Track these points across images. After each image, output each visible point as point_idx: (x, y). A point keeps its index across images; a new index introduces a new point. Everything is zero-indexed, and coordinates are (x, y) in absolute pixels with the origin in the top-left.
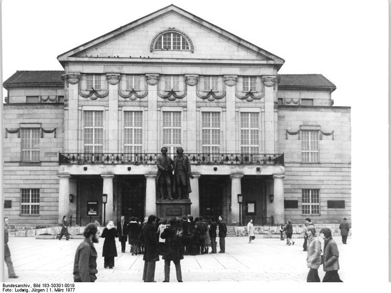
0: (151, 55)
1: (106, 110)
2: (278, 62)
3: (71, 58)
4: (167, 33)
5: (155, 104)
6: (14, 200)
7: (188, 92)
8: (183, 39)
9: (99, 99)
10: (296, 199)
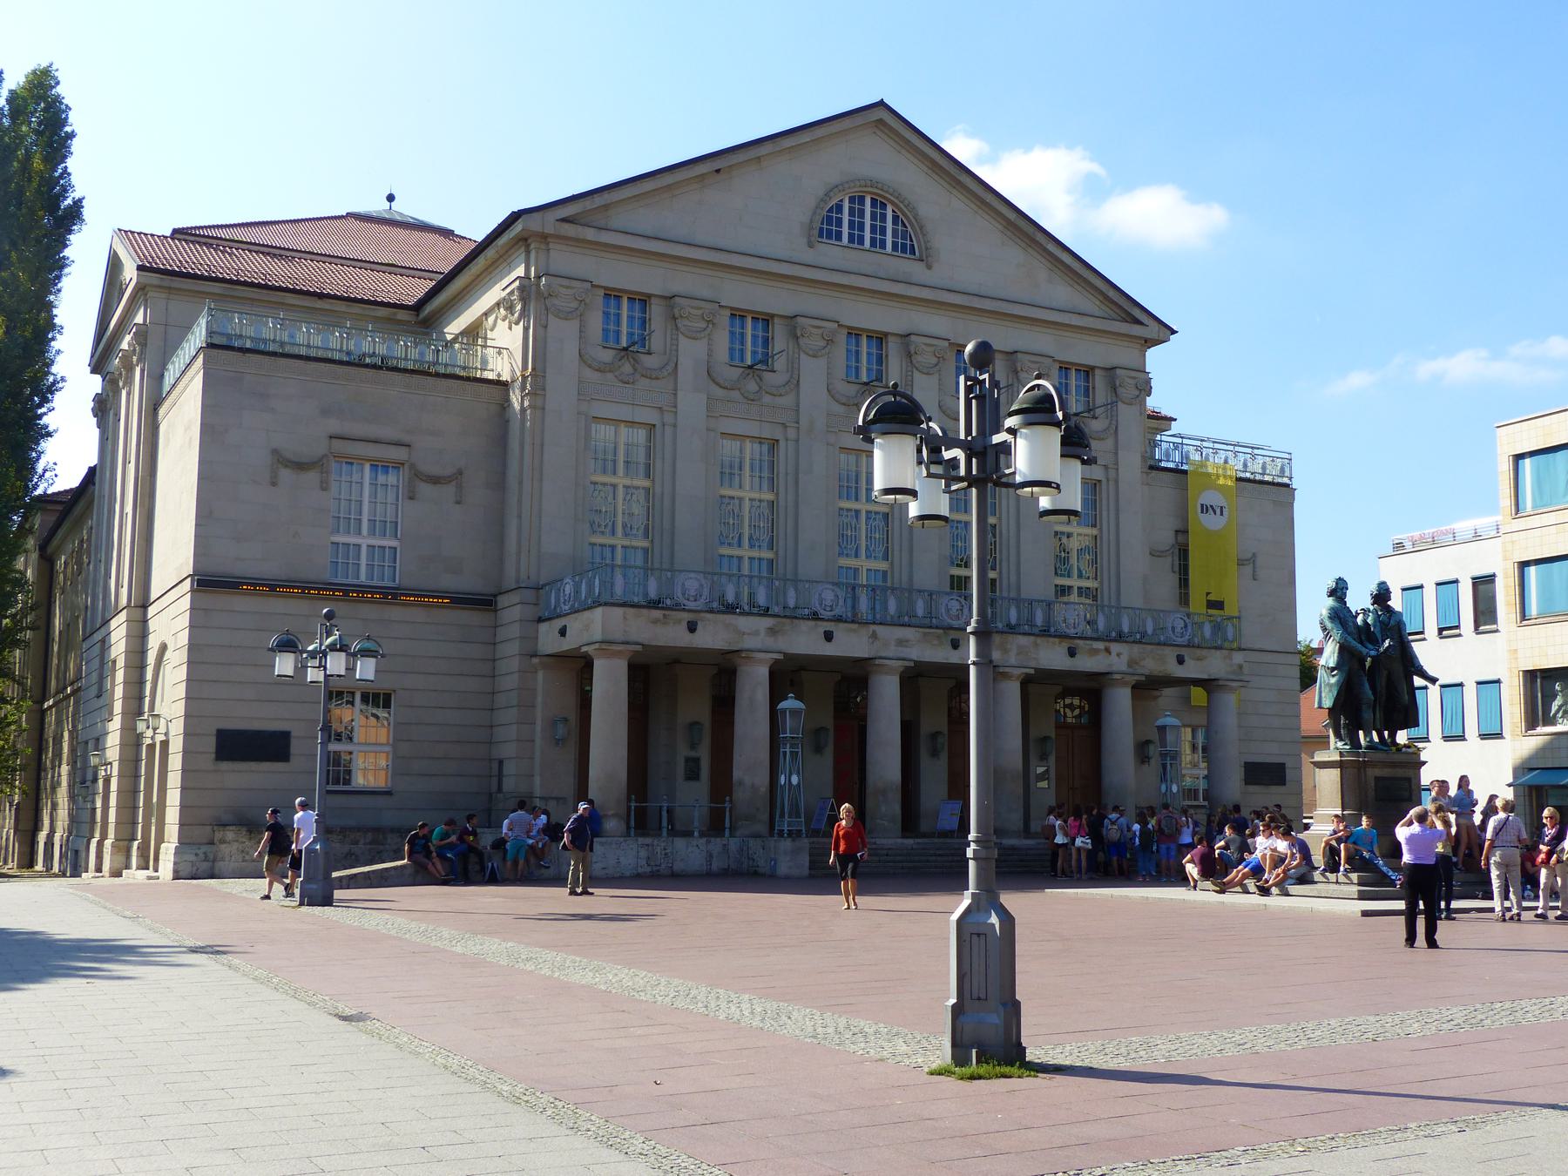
0: (809, 256)
2: (1151, 331)
3: (566, 226)
6: (297, 730)
8: (895, 219)
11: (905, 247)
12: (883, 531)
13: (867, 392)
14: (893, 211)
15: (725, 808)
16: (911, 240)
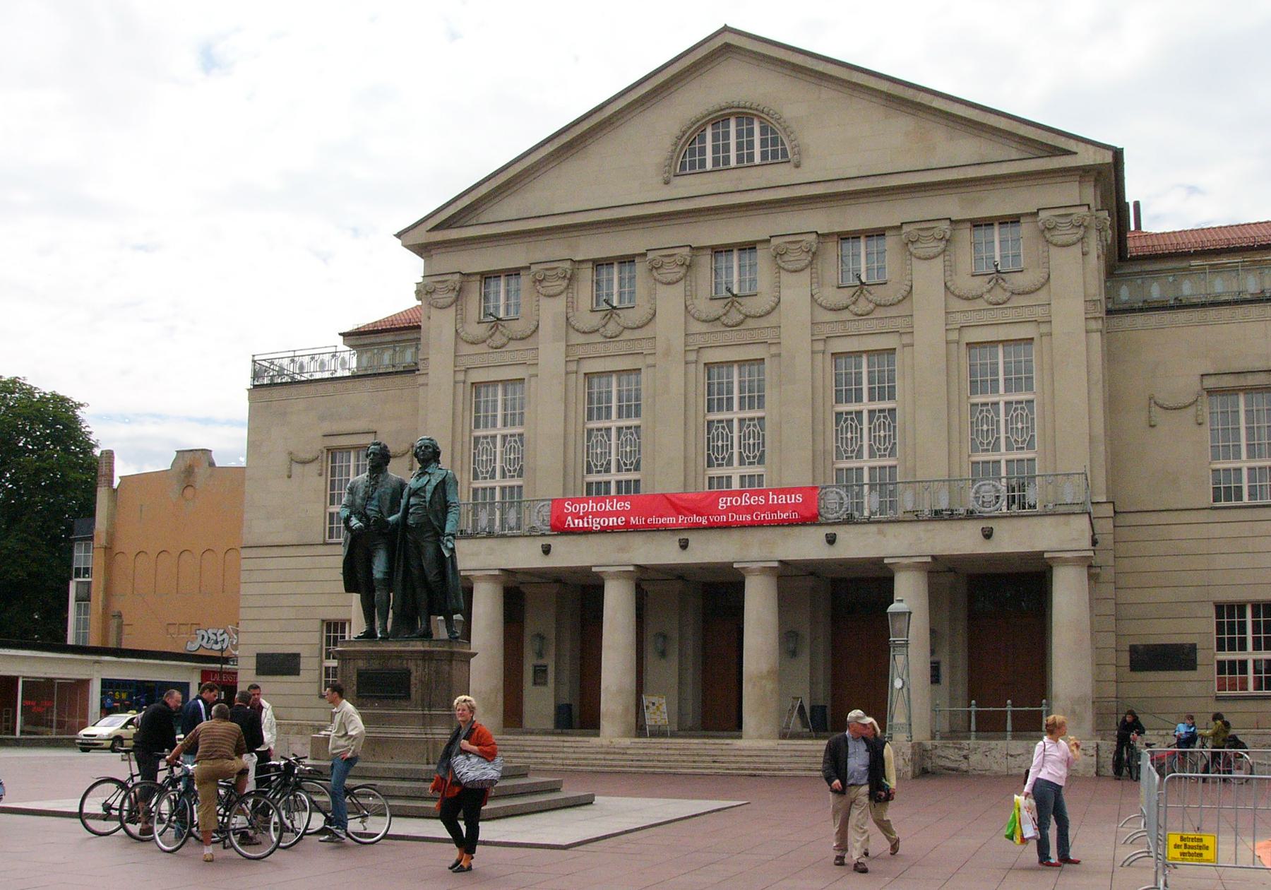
1: (532, 376)
4: (719, 119)
5: (678, 343)
7: (786, 295)
8: (764, 131)
9: (513, 346)
10: (1187, 640)
11: (776, 152)
12: (727, 438)
13: (729, 305)
14: (761, 123)
15: (1006, 712)
16: (783, 144)
